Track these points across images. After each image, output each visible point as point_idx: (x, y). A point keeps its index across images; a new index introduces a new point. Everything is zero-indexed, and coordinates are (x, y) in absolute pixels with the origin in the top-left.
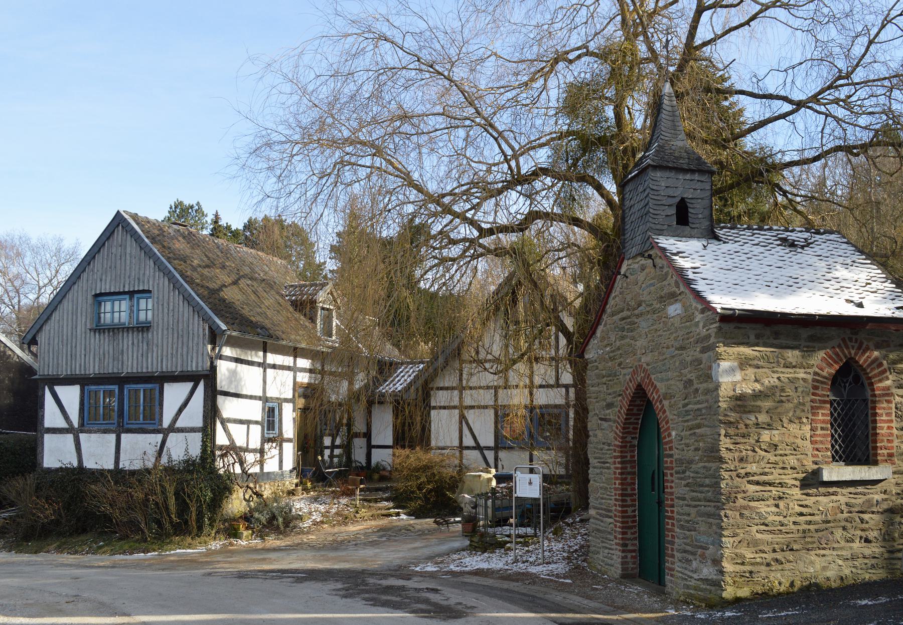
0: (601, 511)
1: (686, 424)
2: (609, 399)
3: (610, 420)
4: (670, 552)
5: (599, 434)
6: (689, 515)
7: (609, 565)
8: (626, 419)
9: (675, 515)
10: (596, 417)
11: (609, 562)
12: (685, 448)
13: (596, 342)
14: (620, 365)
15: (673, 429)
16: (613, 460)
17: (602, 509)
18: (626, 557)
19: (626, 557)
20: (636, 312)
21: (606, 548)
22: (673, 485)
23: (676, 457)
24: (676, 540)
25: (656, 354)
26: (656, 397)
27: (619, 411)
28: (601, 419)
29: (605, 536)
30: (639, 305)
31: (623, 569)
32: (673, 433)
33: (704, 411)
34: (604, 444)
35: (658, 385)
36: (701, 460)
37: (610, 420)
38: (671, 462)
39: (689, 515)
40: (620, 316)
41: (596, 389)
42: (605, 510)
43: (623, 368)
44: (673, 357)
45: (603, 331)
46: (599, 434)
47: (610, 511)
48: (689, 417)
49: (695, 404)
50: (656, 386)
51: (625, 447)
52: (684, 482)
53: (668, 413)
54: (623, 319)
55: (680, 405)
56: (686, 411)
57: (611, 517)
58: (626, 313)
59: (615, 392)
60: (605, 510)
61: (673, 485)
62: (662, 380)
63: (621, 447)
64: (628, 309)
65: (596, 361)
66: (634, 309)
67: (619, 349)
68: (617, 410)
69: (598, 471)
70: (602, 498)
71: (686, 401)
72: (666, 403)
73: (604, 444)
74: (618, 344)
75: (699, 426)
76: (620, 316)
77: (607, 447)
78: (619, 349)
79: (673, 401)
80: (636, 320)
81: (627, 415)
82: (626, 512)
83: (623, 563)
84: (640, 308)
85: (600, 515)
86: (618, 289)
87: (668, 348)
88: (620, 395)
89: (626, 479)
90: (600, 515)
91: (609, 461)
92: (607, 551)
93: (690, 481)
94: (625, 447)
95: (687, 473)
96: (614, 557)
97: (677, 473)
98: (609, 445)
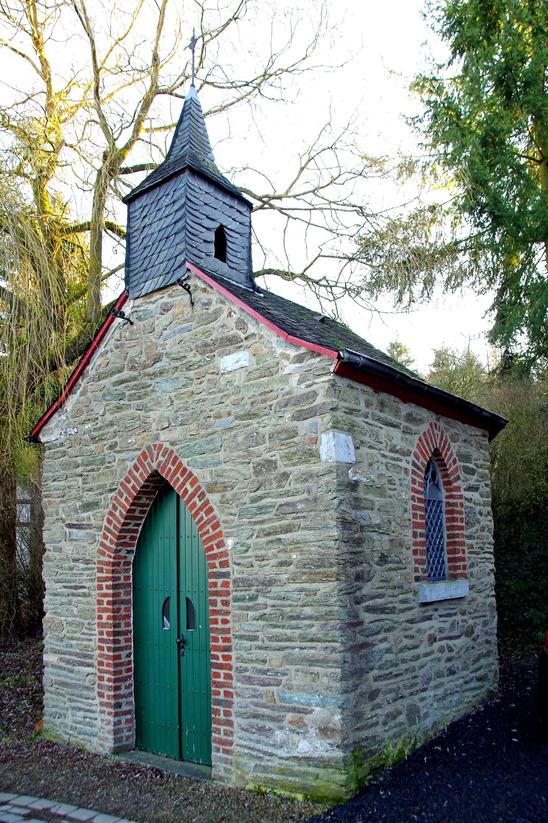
0: (68, 657)
1: (258, 527)
2: (89, 497)
3: (89, 526)
4: (222, 717)
5: (68, 548)
6: (264, 661)
7: (85, 734)
8: (124, 524)
9: (233, 662)
10: (60, 524)
11: (88, 729)
12: (256, 563)
13: (63, 417)
14: (112, 447)
15: (229, 535)
16: (96, 583)
17: (70, 654)
18: (120, 722)
19: (120, 722)
20: (150, 370)
21: (80, 709)
22: (228, 618)
23: (236, 575)
24: (235, 699)
25: (193, 426)
26: (191, 490)
27: (111, 513)
28: (70, 526)
29: (77, 692)
30: (157, 360)
31: (116, 740)
32: (230, 542)
33: (300, 506)
34: (75, 560)
35: (196, 472)
36: (294, 579)
37: (89, 526)
38: (226, 584)
39: (264, 661)
40: (115, 378)
41: (63, 483)
42: (77, 655)
43: (119, 452)
44: (231, 429)
45: (78, 402)
46: (68, 548)
47: (91, 657)
48: (265, 517)
49: (281, 495)
50: (191, 474)
51: (118, 564)
52: (251, 614)
53: (216, 512)
54: (122, 382)
55: (246, 499)
56: (260, 508)
57: (89, 665)
58: (126, 374)
59: (99, 487)
60: (77, 655)
61: (228, 618)
62: (204, 465)
63: (114, 564)
64: (133, 368)
65: (62, 445)
66: (145, 367)
67: (112, 424)
68: (107, 511)
69: (64, 600)
70: (72, 638)
71: (259, 493)
72: (214, 498)
73: (75, 560)
74: (109, 417)
75: (288, 529)
76: (115, 378)
77: (82, 566)
78: (112, 424)
79: (229, 494)
80: (149, 382)
81: (126, 518)
82: (119, 657)
83: (116, 732)
84: (158, 365)
85: (68, 662)
86: (112, 341)
87: (218, 416)
88: (111, 490)
89: (119, 610)
90: (68, 662)
91: (87, 585)
92: (82, 713)
93: (268, 610)
94: (118, 564)
95: (261, 600)
96: (98, 723)
97: (236, 600)
98: (87, 562)
